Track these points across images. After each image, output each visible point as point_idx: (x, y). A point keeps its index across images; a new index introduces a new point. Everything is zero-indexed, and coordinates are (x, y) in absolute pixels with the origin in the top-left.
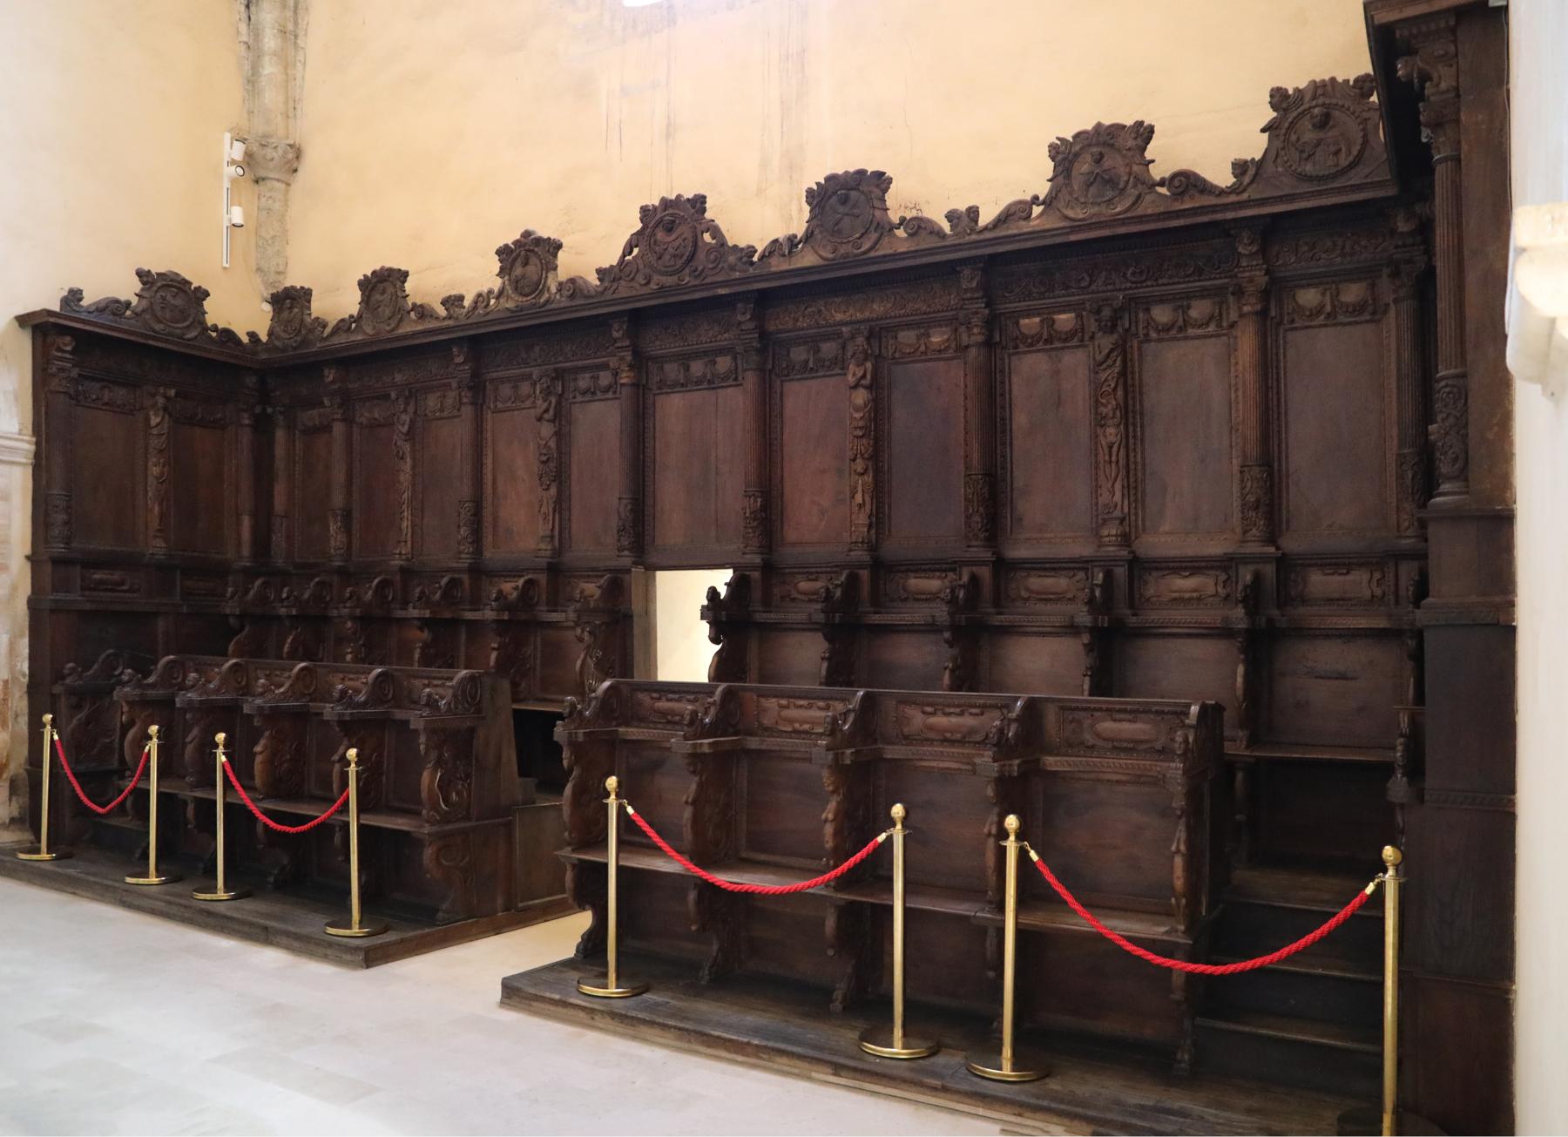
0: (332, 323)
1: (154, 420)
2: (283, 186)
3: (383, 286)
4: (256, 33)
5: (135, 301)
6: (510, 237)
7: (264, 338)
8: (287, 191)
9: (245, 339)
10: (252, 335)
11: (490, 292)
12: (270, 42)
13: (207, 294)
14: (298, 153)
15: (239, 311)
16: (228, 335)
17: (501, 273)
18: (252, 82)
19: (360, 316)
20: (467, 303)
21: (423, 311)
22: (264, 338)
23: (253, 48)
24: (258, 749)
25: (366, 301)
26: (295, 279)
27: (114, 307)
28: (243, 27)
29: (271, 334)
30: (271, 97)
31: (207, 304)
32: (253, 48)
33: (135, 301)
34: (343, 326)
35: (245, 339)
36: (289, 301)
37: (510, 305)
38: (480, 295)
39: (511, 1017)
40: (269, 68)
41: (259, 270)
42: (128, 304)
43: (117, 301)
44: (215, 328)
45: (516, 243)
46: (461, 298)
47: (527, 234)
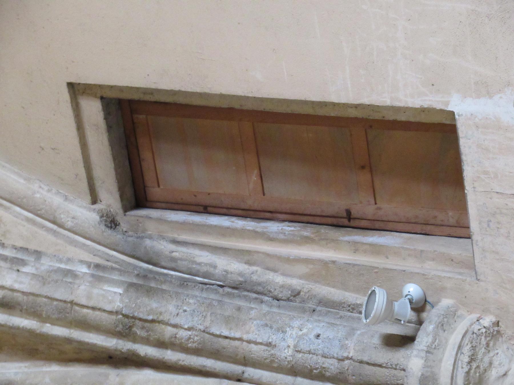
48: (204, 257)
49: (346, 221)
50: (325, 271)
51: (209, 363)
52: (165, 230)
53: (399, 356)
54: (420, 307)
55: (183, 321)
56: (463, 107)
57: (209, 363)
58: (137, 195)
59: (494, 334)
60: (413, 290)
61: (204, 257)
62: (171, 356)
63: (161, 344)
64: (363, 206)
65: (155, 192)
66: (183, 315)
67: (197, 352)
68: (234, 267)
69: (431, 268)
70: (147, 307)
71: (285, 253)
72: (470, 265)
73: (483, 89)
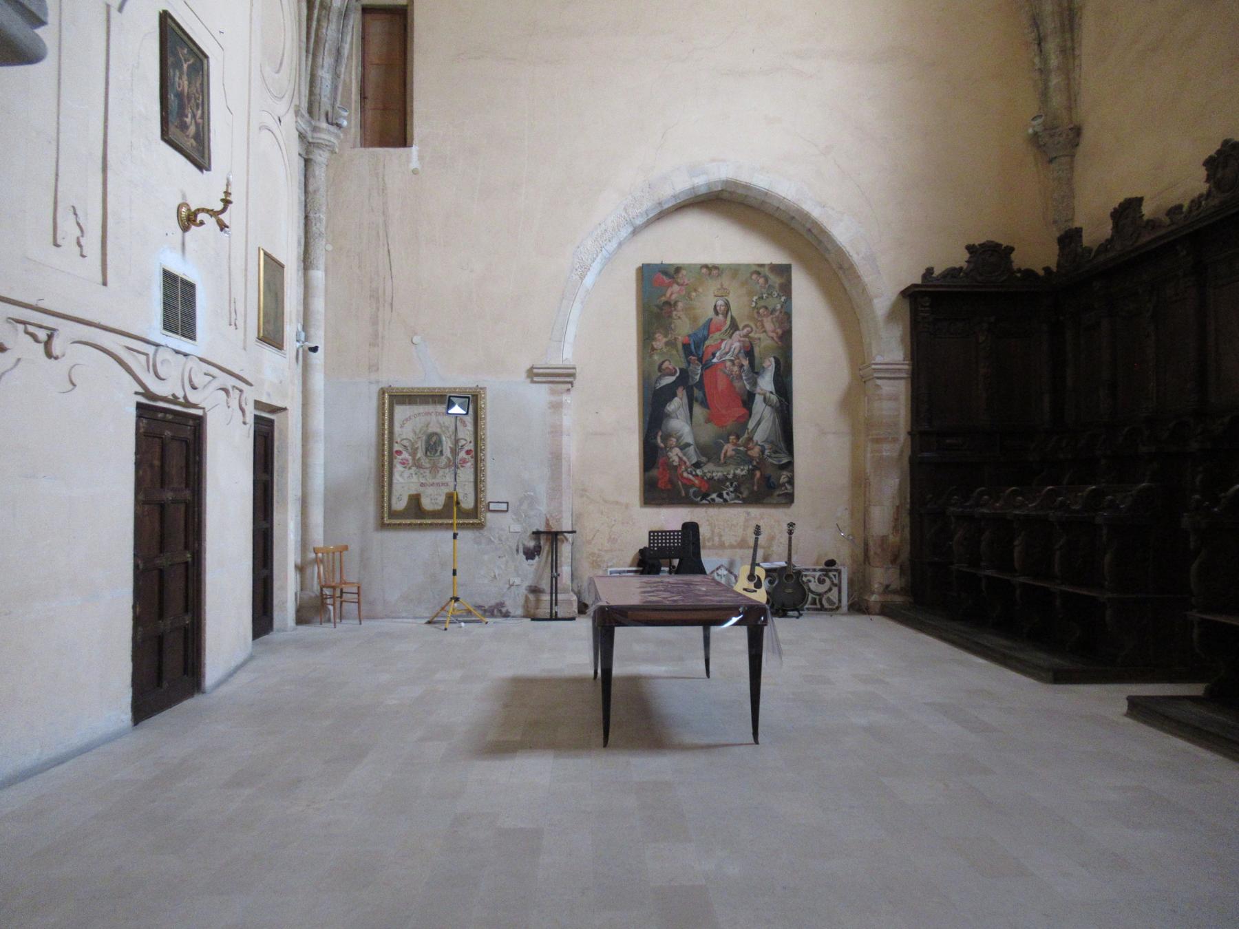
0: (1095, 248)
1: (982, 338)
2: (1068, 159)
3: (1127, 211)
4: (1045, 60)
5: (965, 265)
6: (1213, 148)
7: (1054, 269)
8: (1072, 161)
9: (1041, 273)
10: (1047, 269)
11: (1201, 196)
12: (1054, 62)
13: (1012, 249)
14: (1077, 131)
15: (1036, 254)
16: (1029, 273)
17: (1208, 180)
18: (1044, 95)
19: (1112, 236)
20: (1185, 209)
21: (1153, 224)
22: (1054, 269)
23: (1044, 71)
24: (1016, 543)
25: (1116, 227)
26: (1077, 224)
27: (952, 273)
28: (1037, 60)
29: (1058, 265)
30: (1057, 100)
31: (1013, 256)
32: (1044, 71)
33: (965, 265)
34: (1105, 247)
35: (1041, 273)
36: (1069, 239)
37: (1216, 202)
38: (1193, 201)
39: (1128, 720)
40: (1055, 80)
41: (1055, 222)
42: (961, 268)
43: (954, 269)
44: (1019, 270)
45: (1219, 152)
46: (1180, 207)
47: (1226, 143)
48: (348, 39)
49: (363, 97)
50: (347, 89)
51: (312, 40)
52: (355, 19)
53: (323, 118)
54: (339, 126)
55: (329, 32)
56: (414, 150)
57: (312, 40)
58: (366, 10)
59: (333, 152)
60: (345, 123)
61: (348, 39)
62: (314, 24)
63: (319, 21)
64: (370, 104)
65: (368, 17)
66: (330, 32)
67: (317, 35)
68: (346, 52)
69: (353, 130)
70: (334, 17)
71: (351, 73)
72: (354, 147)
73: (421, 158)
